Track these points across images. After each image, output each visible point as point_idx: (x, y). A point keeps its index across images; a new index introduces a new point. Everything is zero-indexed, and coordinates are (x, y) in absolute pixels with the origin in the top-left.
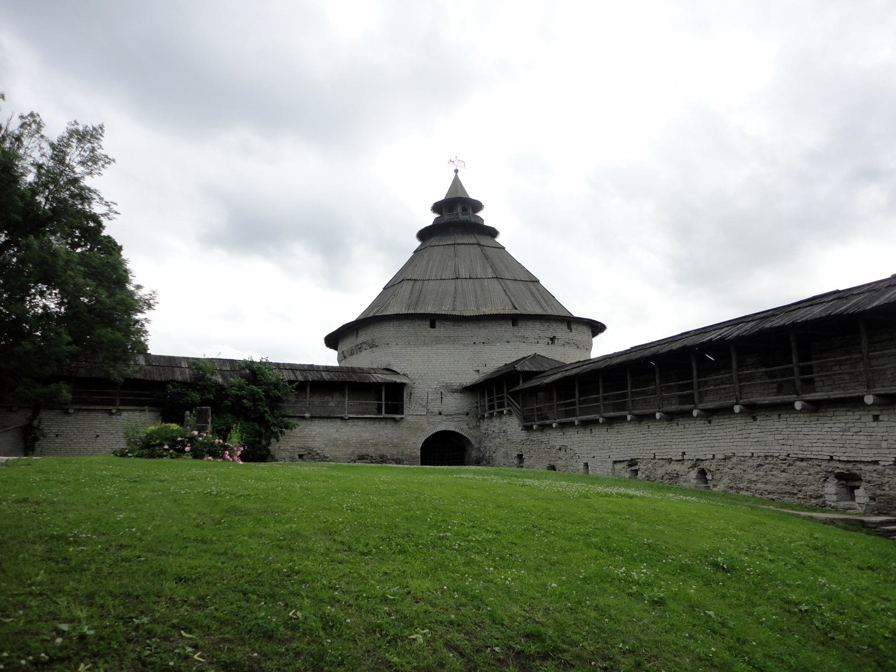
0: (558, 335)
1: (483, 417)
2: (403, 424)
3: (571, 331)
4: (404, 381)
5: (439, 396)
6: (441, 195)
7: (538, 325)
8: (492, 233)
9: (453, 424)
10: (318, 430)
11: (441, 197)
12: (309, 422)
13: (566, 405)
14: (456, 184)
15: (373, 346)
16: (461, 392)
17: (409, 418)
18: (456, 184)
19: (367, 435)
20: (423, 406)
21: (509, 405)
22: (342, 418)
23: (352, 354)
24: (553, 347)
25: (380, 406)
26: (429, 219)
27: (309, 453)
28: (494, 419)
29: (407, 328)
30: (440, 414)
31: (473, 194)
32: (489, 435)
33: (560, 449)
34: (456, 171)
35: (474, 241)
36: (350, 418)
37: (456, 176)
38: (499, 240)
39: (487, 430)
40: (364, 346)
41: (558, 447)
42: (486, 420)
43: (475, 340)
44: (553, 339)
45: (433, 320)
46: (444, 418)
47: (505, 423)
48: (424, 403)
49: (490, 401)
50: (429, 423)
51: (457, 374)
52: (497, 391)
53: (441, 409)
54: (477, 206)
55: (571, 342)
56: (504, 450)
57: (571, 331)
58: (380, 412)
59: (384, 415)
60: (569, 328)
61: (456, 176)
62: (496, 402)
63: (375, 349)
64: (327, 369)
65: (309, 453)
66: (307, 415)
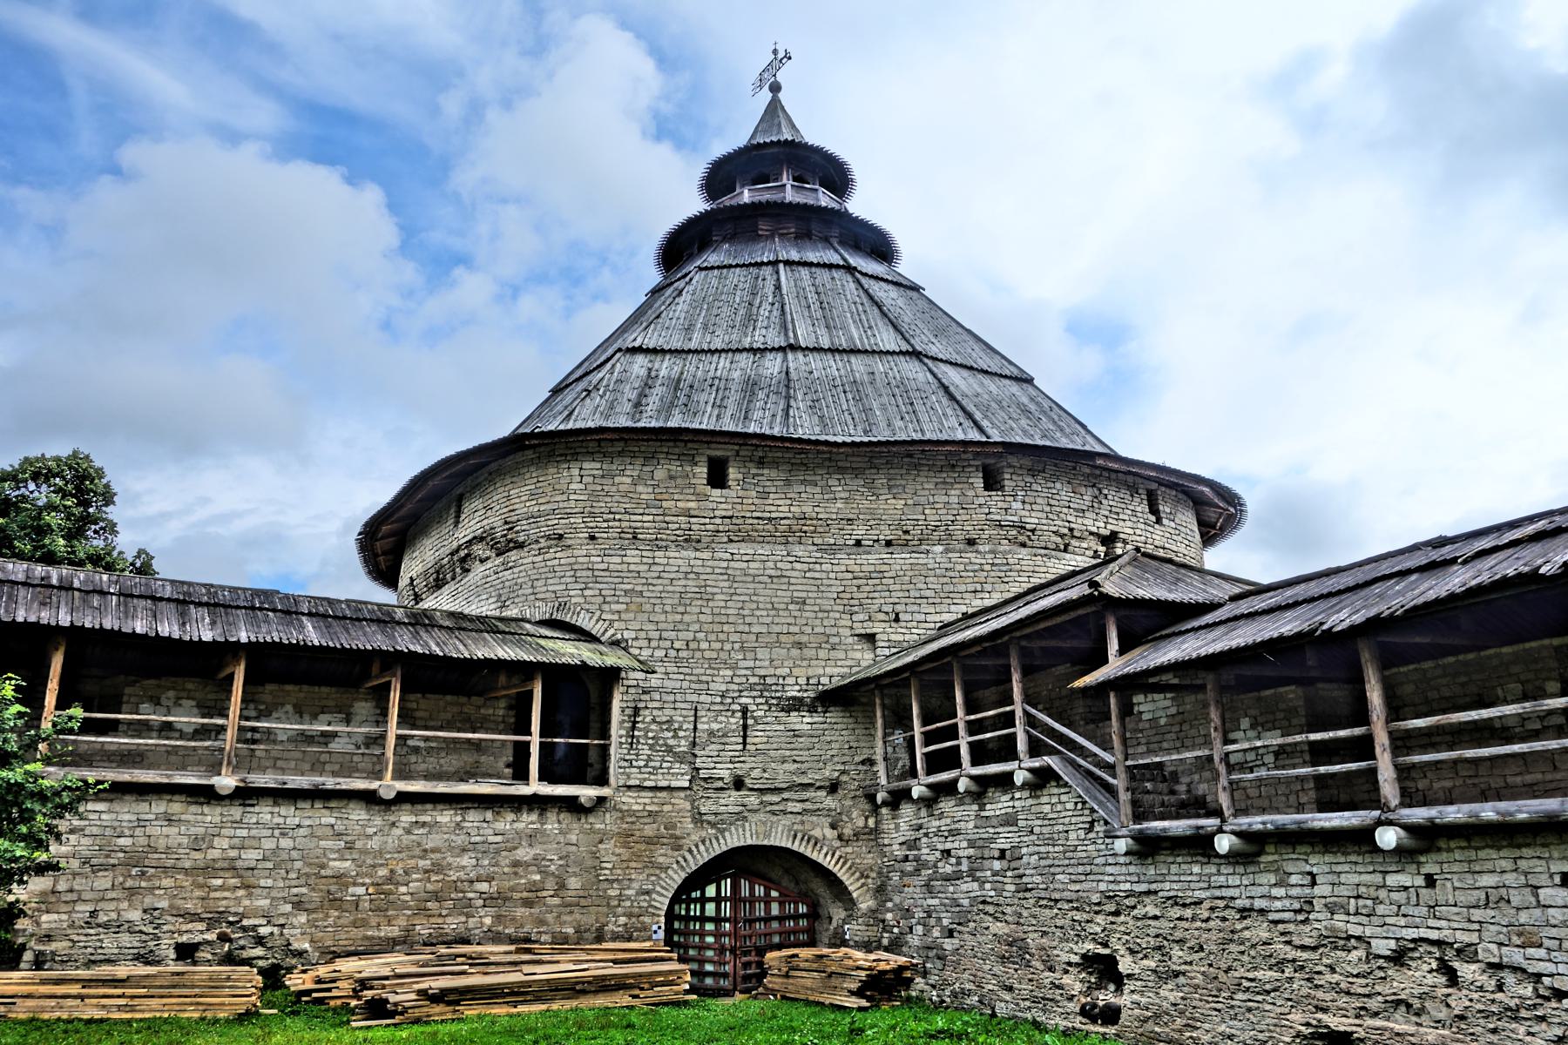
0: (1125, 529)
1: (899, 797)
2: (604, 822)
4: (612, 659)
5: (736, 721)
9: (786, 821)
10: (269, 844)
12: (236, 812)
13: (1320, 753)
15: (506, 545)
16: (812, 709)
17: (630, 800)
19: (466, 860)
20: (680, 758)
21: (1036, 749)
22: (369, 798)
23: (439, 584)
25: (522, 750)
27: (223, 938)
28: (947, 805)
29: (628, 482)
30: (739, 784)
32: (921, 865)
33: (1399, 958)
34: (775, 88)
35: (835, 258)
36: (403, 798)
39: (912, 844)
40: (479, 550)
41: (1383, 947)
42: (907, 810)
43: (860, 531)
45: (720, 454)
46: (753, 800)
47: (1010, 820)
48: (683, 746)
49: (929, 738)
50: (698, 818)
51: (799, 645)
52: (944, 704)
53: (741, 769)
54: (836, 176)
56: (999, 928)
57: (1159, 521)
58: (521, 775)
59: (535, 787)
60: (1154, 510)
62: (963, 743)
63: (513, 555)
64: (327, 612)
65: (223, 938)
66: (226, 782)
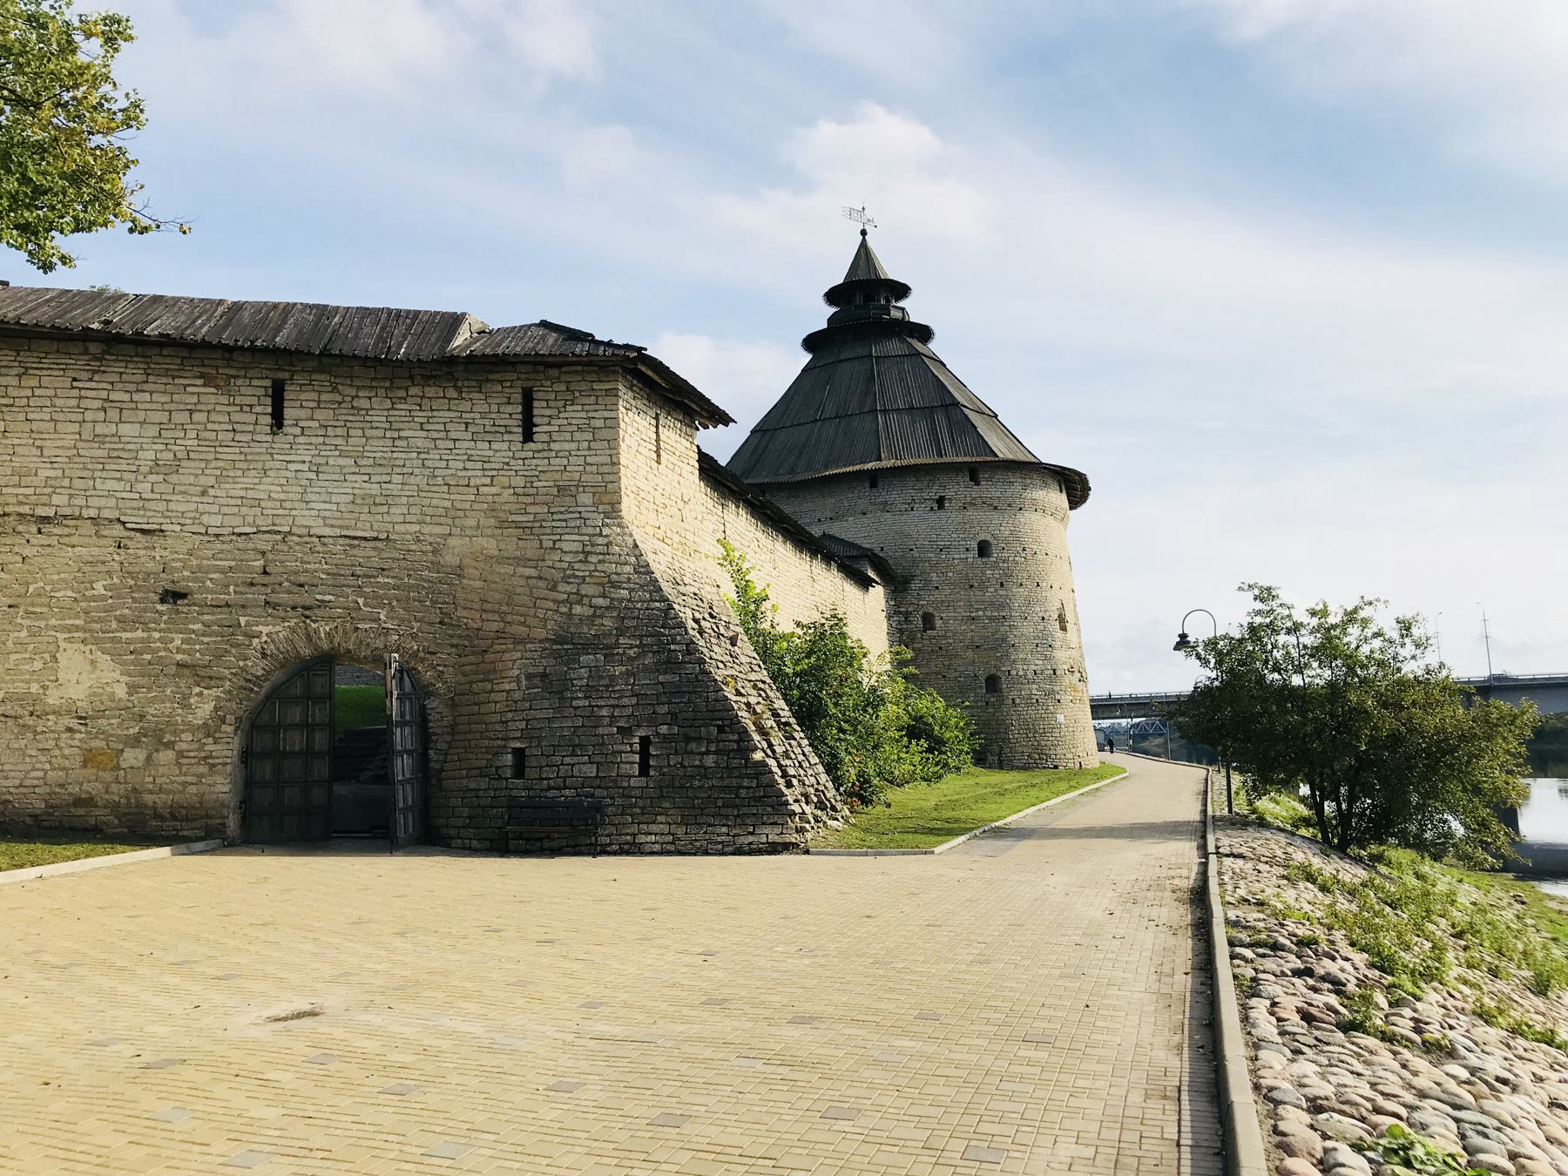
0: (949, 494)
3: (978, 484)
6: (837, 276)
7: (911, 481)
8: (925, 333)
11: (839, 280)
14: (864, 255)
18: (864, 255)
24: (942, 514)
26: (820, 316)
31: (890, 268)
37: (864, 245)
38: (934, 346)
44: (941, 502)
54: (902, 291)
55: (979, 501)
61: (864, 245)
